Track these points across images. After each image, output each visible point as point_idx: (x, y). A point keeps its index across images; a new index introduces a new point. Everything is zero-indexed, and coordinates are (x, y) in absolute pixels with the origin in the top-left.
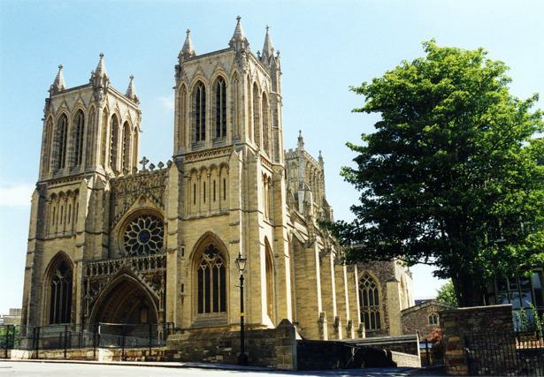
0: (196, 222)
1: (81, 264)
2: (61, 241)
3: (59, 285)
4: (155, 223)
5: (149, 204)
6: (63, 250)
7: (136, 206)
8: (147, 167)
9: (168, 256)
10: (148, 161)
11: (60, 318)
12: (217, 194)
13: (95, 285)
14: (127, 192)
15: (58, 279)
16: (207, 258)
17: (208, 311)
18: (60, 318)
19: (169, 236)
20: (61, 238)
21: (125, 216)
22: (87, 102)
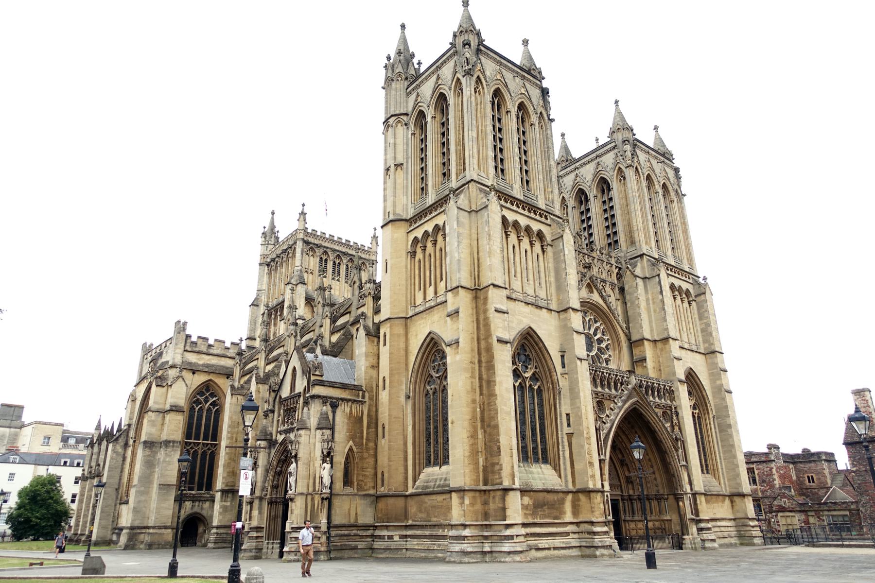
4: (598, 327)
5: (596, 297)
11: (530, 454)
18: (530, 454)
20: (527, 303)
22: (534, 100)
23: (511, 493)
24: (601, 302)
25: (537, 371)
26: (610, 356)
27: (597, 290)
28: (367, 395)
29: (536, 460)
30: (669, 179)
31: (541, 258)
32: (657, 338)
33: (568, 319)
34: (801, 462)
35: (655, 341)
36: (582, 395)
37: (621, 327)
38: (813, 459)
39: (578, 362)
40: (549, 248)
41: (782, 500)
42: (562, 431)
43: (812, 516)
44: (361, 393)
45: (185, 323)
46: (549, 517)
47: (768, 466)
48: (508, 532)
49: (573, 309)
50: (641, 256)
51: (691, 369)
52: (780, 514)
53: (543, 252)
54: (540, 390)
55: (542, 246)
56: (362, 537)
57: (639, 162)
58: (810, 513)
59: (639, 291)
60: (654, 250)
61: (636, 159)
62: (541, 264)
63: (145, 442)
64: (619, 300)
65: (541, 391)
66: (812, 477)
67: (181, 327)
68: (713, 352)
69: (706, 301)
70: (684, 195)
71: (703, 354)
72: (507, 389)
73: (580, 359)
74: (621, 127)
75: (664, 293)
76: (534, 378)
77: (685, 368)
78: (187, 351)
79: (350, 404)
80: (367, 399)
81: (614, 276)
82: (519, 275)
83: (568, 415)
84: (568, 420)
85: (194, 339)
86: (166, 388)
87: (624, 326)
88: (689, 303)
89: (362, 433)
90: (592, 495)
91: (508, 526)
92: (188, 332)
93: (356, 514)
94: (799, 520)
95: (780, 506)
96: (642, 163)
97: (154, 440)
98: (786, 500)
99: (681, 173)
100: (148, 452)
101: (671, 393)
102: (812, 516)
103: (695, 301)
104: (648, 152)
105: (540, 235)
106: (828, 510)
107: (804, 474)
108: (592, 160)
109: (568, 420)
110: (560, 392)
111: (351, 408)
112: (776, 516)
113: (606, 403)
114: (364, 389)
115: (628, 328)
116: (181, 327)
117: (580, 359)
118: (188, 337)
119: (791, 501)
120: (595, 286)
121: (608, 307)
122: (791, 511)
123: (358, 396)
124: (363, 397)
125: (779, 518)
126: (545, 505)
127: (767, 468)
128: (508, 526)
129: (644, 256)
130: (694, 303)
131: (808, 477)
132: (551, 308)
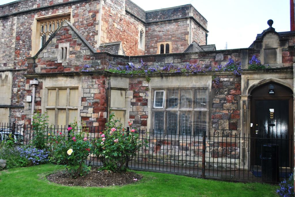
34: (156, 23)
38: (175, 17)
41: (61, 46)
43: (121, 89)
47: (93, 8)
52: (47, 83)
58: (114, 82)
66: (168, 46)
94: (83, 99)
95: (51, 62)
98: (67, 45)
102: (121, 89)
106: (162, 75)
107: (157, 42)
112: (38, 87)
119: (78, 48)
122: (70, 75)
125: (43, 92)
127: (89, 12)
131: (162, 46)
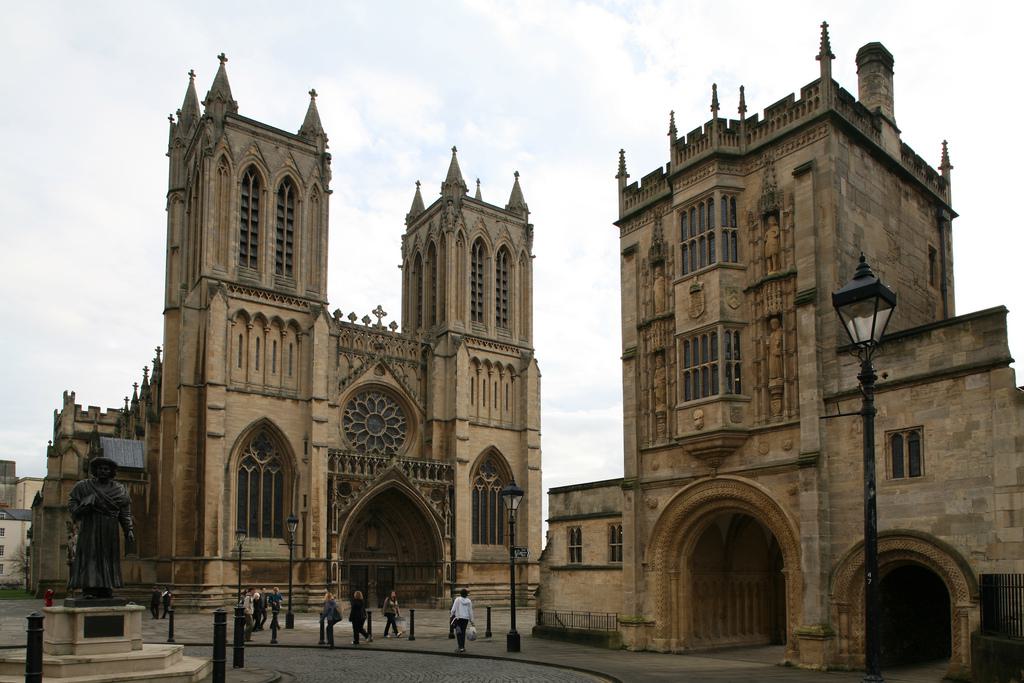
0: (478, 428)
1: (324, 452)
2: (266, 401)
3: (256, 473)
4: (392, 409)
5: (387, 379)
6: (271, 417)
7: (369, 376)
8: (386, 322)
9: (459, 468)
10: (385, 314)
12: (498, 400)
13: (345, 489)
14: (357, 352)
15: (255, 462)
16: (483, 475)
17: (486, 543)
19: (458, 442)
20: (265, 396)
21: (353, 387)
23: (212, 563)
24: (394, 383)
25: (277, 457)
26: (403, 436)
27: (390, 371)
28: (149, 476)
29: (267, 534)
30: (511, 240)
31: (295, 348)
32: (448, 419)
33: (311, 408)
35: (446, 421)
36: (314, 479)
37: (418, 407)
39: (315, 450)
40: (304, 338)
42: (297, 509)
44: (142, 475)
45: (73, 394)
46: (269, 581)
48: (204, 592)
49: (316, 399)
50: (446, 333)
51: (493, 447)
53: (298, 341)
54: (280, 476)
55: (297, 336)
56: (144, 593)
57: (464, 226)
59: (437, 370)
60: (467, 326)
61: (460, 221)
62: (295, 353)
63: (45, 508)
64: (419, 380)
65: (281, 475)
67: (69, 399)
68: (526, 430)
69: (527, 377)
70: (534, 257)
71: (518, 431)
72: (216, 479)
73: (318, 447)
74: (454, 183)
75: (459, 373)
76: (273, 463)
77: (485, 447)
78: (78, 421)
79: (130, 484)
80: (149, 480)
81: (419, 353)
82: (261, 368)
83: (305, 496)
84: (305, 500)
85: (85, 408)
86: (59, 458)
87: (421, 405)
88: (512, 378)
89: (145, 505)
90: (313, 564)
91: (206, 588)
92: (76, 403)
93: (140, 576)
96: (469, 226)
97: (53, 505)
99: (536, 230)
100: (49, 516)
101: (451, 473)
103: (519, 376)
104: (482, 211)
105: (293, 324)
108: (427, 220)
109: (305, 500)
110: (299, 477)
111: (132, 487)
113: (353, 485)
114: (146, 471)
115: (425, 408)
116: (69, 399)
117: (318, 447)
118: (80, 406)
120: (388, 368)
121: (403, 388)
123: (140, 478)
124: (145, 478)
126: (265, 571)
128: (206, 588)
129: (449, 334)
130: (517, 379)
132: (299, 397)
